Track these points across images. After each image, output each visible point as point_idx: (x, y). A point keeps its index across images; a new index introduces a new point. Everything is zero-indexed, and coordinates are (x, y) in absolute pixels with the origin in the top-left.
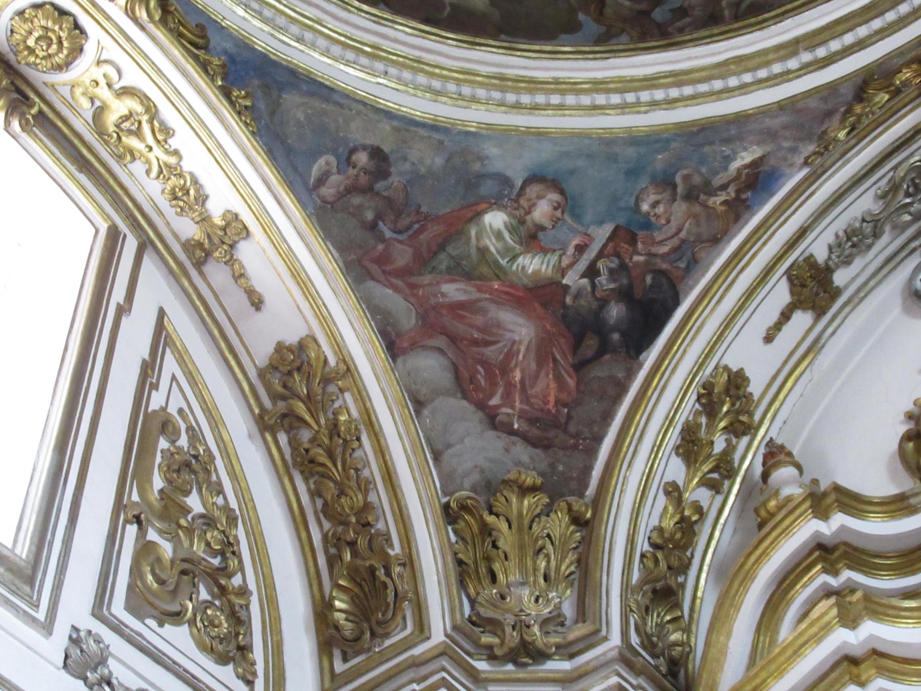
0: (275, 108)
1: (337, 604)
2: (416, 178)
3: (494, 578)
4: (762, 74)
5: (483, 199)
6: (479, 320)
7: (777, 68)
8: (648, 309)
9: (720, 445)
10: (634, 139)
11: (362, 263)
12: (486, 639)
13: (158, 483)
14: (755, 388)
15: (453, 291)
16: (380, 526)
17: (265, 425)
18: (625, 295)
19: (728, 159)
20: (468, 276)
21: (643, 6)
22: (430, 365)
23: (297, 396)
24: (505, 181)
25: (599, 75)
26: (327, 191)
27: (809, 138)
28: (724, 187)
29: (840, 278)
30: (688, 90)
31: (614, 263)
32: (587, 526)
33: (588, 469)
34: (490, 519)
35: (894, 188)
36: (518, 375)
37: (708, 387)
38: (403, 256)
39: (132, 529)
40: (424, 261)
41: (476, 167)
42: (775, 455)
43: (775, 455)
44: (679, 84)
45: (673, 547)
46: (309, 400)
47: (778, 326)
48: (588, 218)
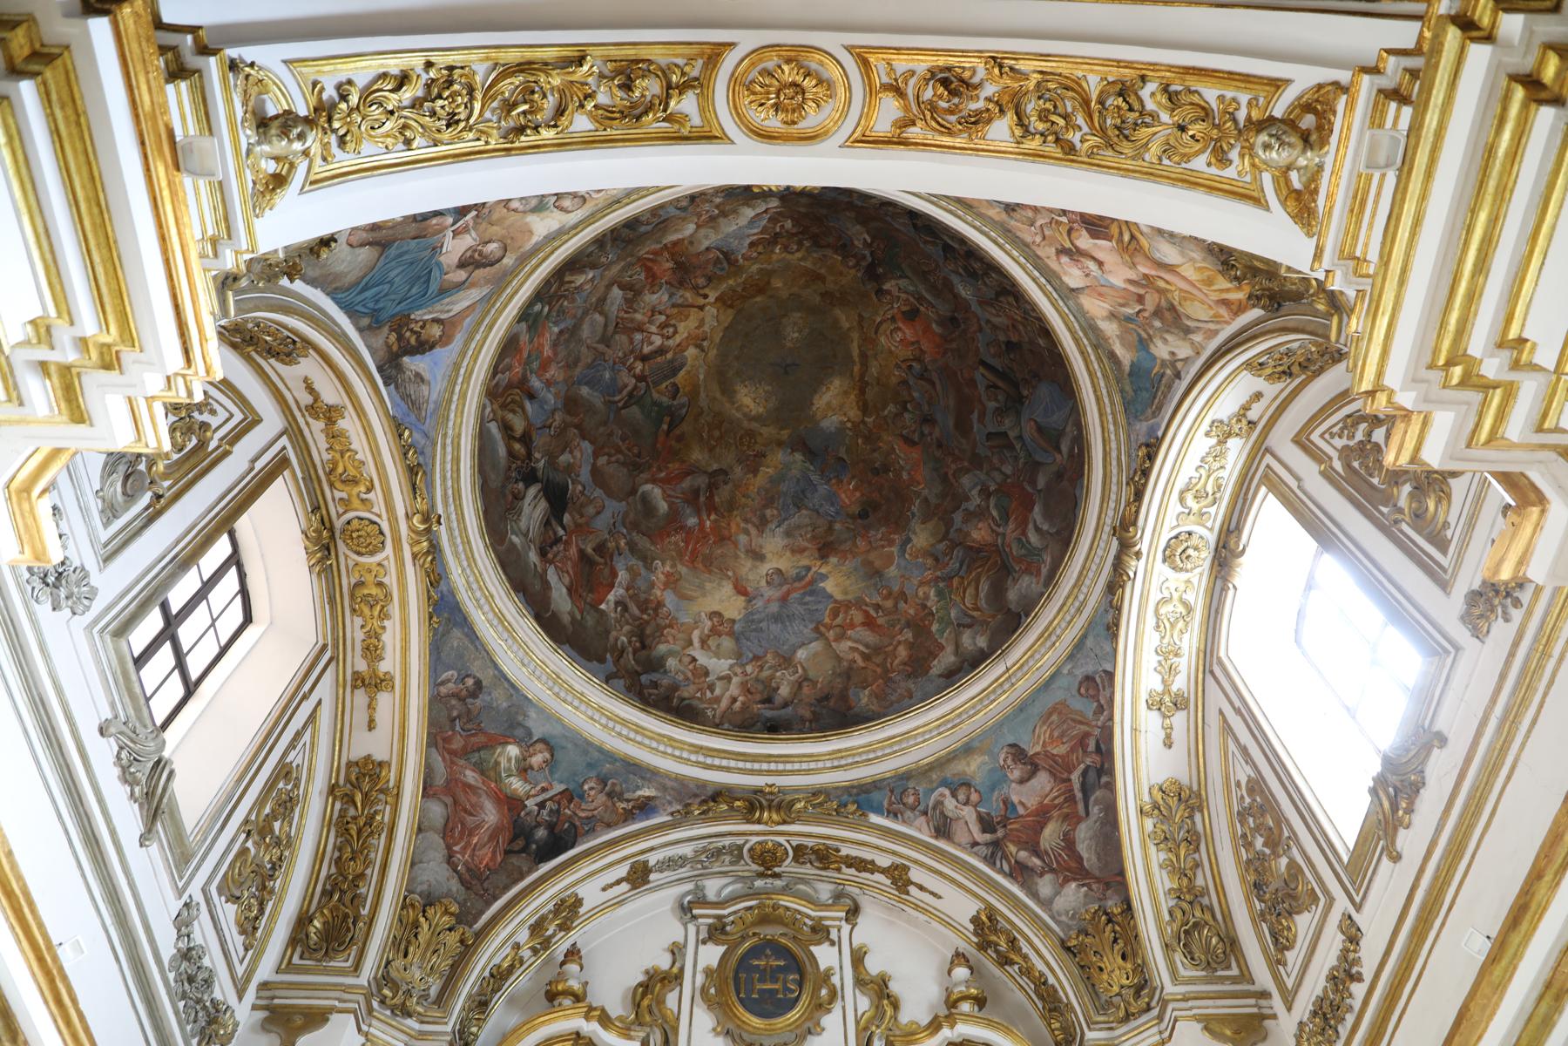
0: (447, 633)
1: (316, 923)
2: (489, 707)
3: (406, 956)
5: (513, 736)
6: (474, 799)
7: (685, 755)
9: (550, 932)
10: (601, 750)
11: (436, 737)
12: (386, 992)
13: (267, 810)
14: (582, 910)
15: (471, 776)
16: (363, 890)
17: (332, 789)
18: (551, 827)
19: (638, 788)
20: (482, 773)
22: (437, 811)
23: (361, 785)
24: (530, 734)
25: (603, 704)
26: (443, 690)
27: (680, 801)
28: (628, 801)
29: (652, 877)
30: (639, 738)
31: (555, 807)
32: (467, 950)
33: (482, 912)
34: (422, 920)
35: (704, 850)
37: (563, 901)
38: (457, 744)
39: (244, 836)
40: (465, 753)
41: (520, 718)
42: (573, 954)
43: (573, 954)
44: (637, 732)
45: (499, 977)
46: (366, 796)
47: (611, 886)
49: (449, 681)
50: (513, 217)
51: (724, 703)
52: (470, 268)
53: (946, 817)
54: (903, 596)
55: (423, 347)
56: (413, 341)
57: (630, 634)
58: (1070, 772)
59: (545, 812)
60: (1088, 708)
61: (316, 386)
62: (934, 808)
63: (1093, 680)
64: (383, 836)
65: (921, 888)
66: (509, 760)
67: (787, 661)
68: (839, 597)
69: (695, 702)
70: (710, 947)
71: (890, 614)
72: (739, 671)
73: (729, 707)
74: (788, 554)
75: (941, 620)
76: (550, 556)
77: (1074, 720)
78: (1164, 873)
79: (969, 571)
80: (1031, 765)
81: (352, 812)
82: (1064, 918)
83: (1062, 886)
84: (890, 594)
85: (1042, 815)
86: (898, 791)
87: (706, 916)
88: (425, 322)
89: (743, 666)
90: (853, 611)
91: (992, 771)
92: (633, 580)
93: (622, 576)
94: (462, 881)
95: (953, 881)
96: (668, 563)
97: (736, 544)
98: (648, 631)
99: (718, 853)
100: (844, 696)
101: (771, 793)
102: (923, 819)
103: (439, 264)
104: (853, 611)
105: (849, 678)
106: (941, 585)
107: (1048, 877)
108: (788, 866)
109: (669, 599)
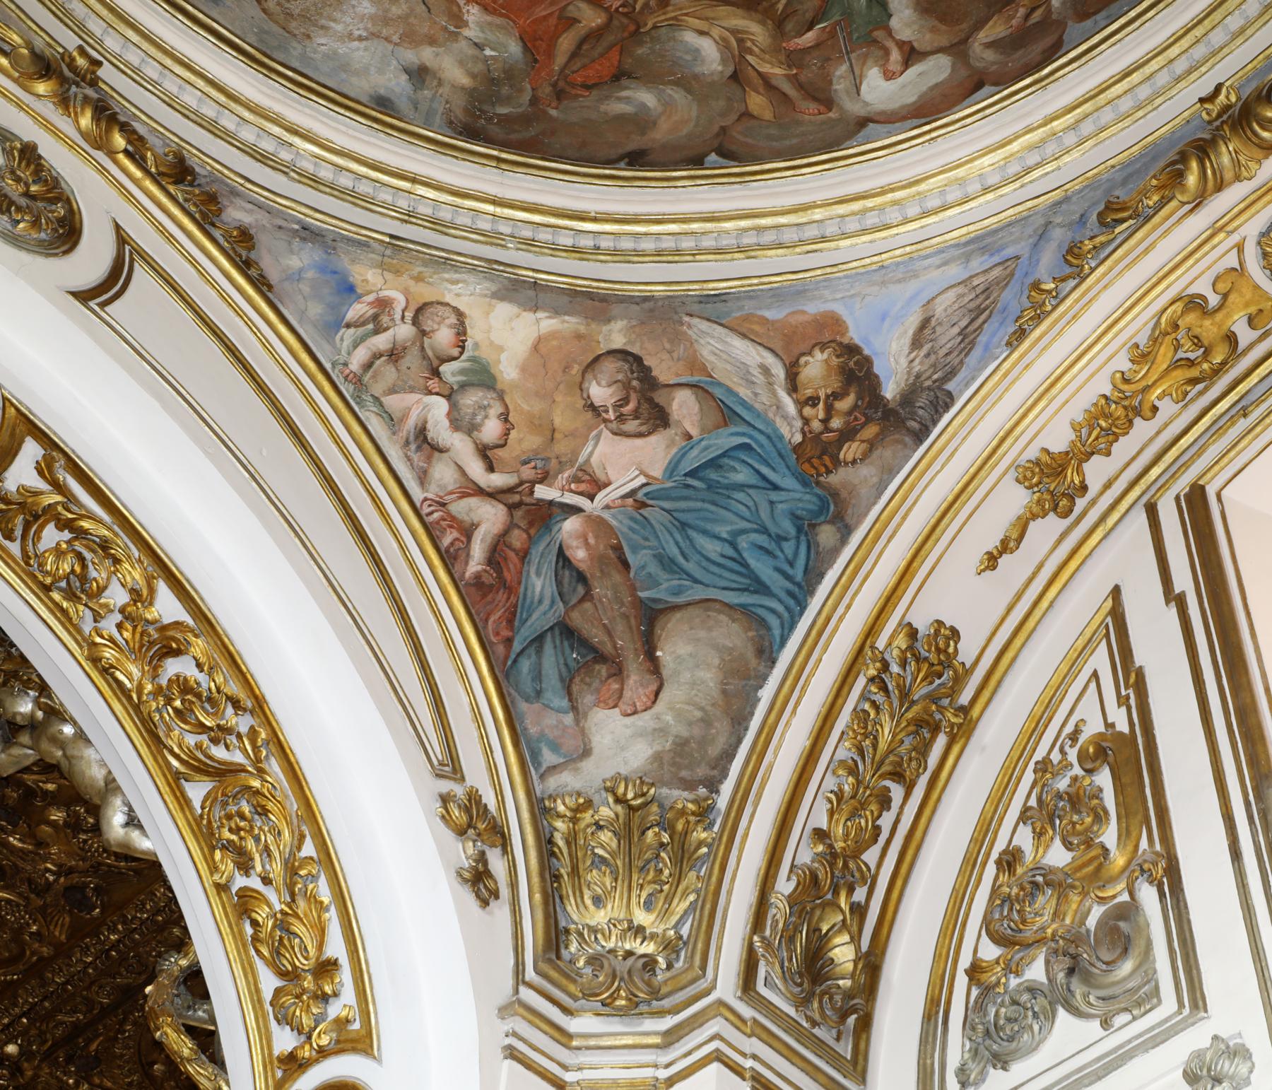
50: (521, 405)
52: (660, 397)
55: (856, 370)
56: (844, 405)
61: (992, 543)
88: (801, 404)
103: (671, 469)
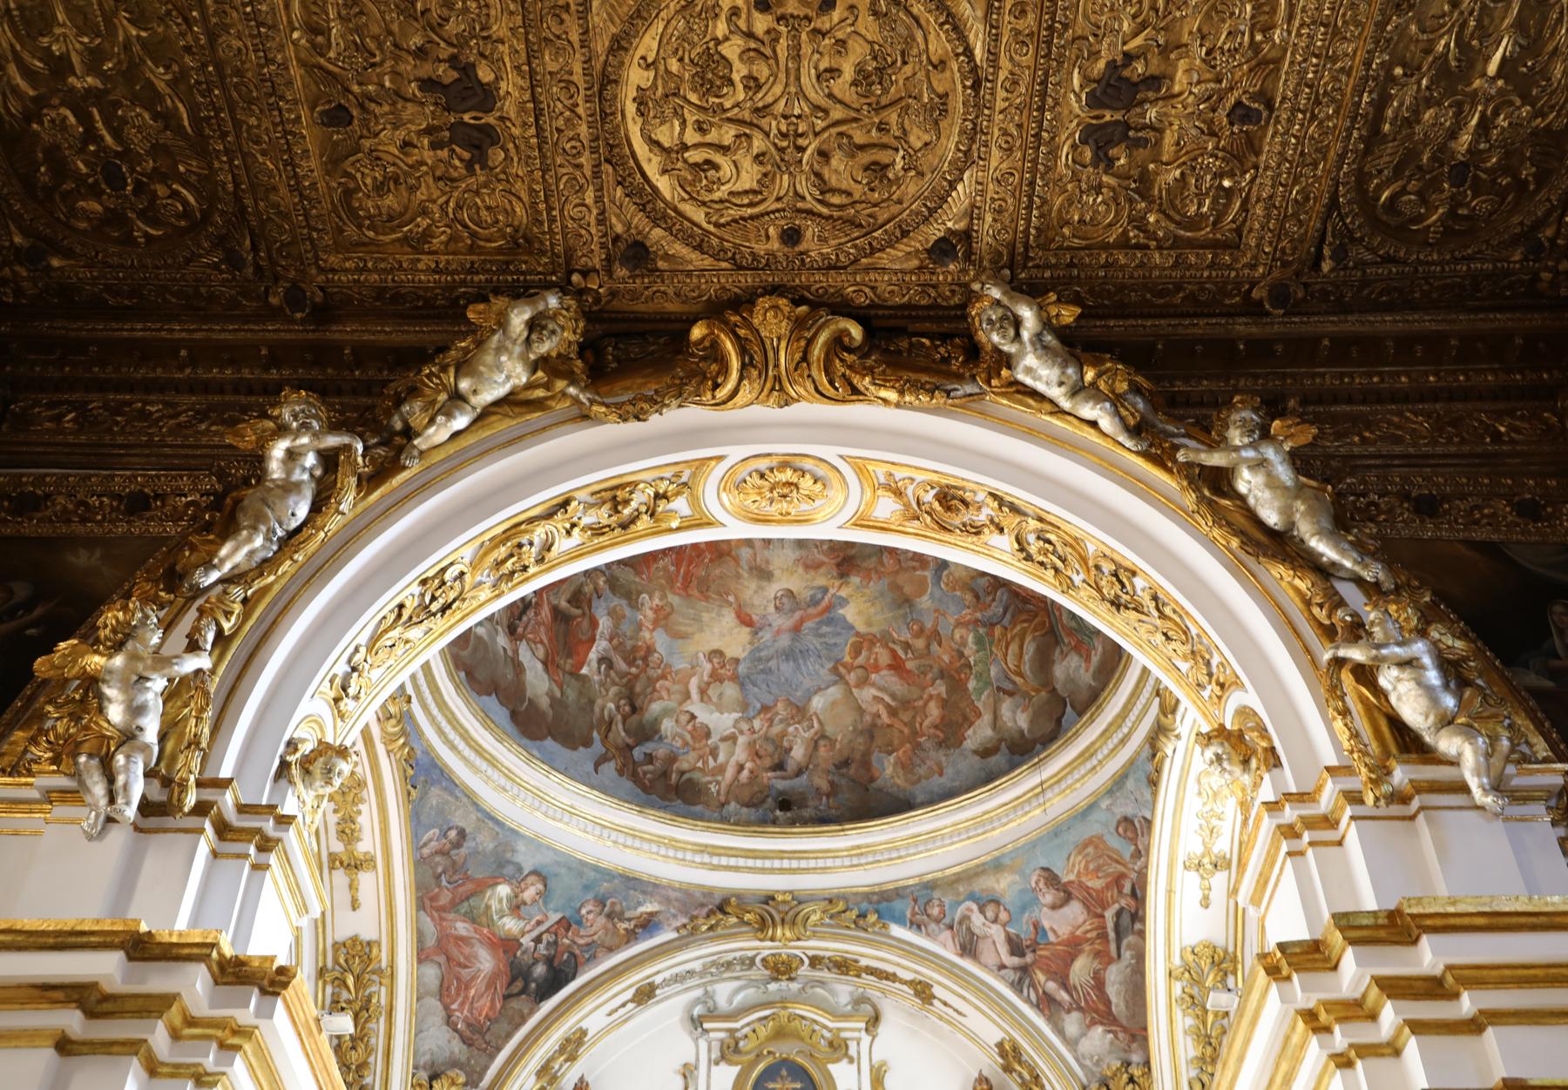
2: (475, 852)
4: (680, 855)
5: (503, 876)
6: (467, 950)
8: (558, 977)
11: (425, 900)
15: (462, 928)
16: (368, 1080)
17: (321, 972)
18: (549, 961)
19: (640, 904)
20: (474, 921)
21: (630, 741)
22: (432, 973)
24: (520, 869)
27: (685, 913)
28: (629, 920)
31: (552, 938)
33: (486, 1068)
35: (713, 963)
36: (472, 992)
38: (445, 899)
40: (454, 905)
41: (508, 855)
46: (358, 979)
48: (551, 906)
49: (431, 840)
51: (730, 772)
53: (973, 934)
54: (935, 635)
57: (619, 696)
58: (1104, 909)
59: (541, 946)
60: (1127, 851)
62: (960, 923)
63: (1132, 823)
64: (382, 1020)
65: (945, 1004)
66: (500, 901)
67: (800, 712)
68: (862, 629)
69: (696, 775)
70: (723, 1066)
71: (921, 657)
72: (745, 727)
73: (736, 779)
74: (801, 570)
75: (979, 677)
76: (520, 630)
77: (1110, 858)
78: (1189, 1039)
79: (1014, 622)
80: (1066, 894)
81: (345, 995)
82: (1088, 1062)
83: (1089, 1027)
84: (921, 632)
85: (1073, 946)
86: (921, 901)
87: (718, 1031)
89: (750, 720)
90: (878, 649)
91: (1023, 891)
92: (616, 625)
93: (604, 623)
94: (464, 1040)
95: (977, 1008)
96: (657, 594)
97: (737, 560)
98: (638, 689)
99: (729, 965)
100: (866, 764)
101: (784, 902)
102: (948, 933)
104: (878, 649)
105: (872, 737)
106: (982, 630)
107: (1075, 1015)
108: (805, 970)
109: (660, 640)
